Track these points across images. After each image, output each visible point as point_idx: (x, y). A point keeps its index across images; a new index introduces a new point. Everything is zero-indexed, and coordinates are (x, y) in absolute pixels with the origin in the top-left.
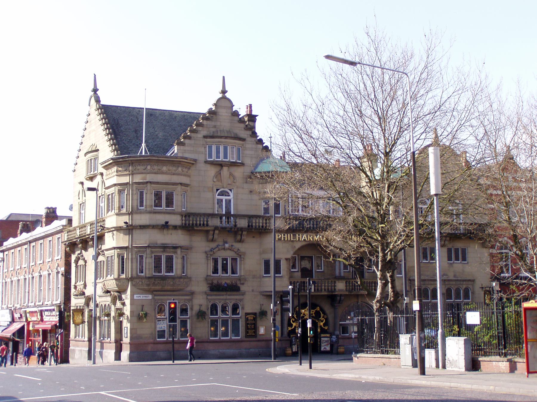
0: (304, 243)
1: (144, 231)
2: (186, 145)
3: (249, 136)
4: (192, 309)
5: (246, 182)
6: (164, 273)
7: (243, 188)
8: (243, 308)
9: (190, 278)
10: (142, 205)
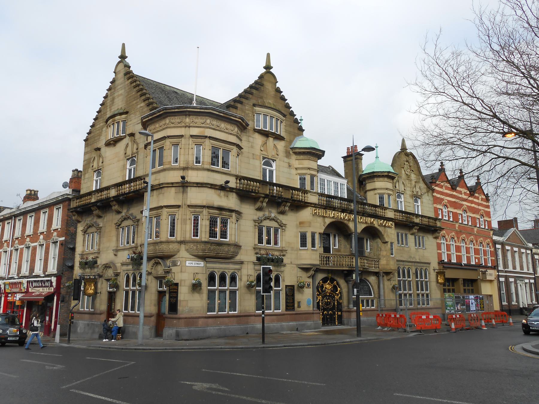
0: (333, 220)
1: (202, 189)
2: (238, 109)
8: (284, 280)
9: (240, 246)
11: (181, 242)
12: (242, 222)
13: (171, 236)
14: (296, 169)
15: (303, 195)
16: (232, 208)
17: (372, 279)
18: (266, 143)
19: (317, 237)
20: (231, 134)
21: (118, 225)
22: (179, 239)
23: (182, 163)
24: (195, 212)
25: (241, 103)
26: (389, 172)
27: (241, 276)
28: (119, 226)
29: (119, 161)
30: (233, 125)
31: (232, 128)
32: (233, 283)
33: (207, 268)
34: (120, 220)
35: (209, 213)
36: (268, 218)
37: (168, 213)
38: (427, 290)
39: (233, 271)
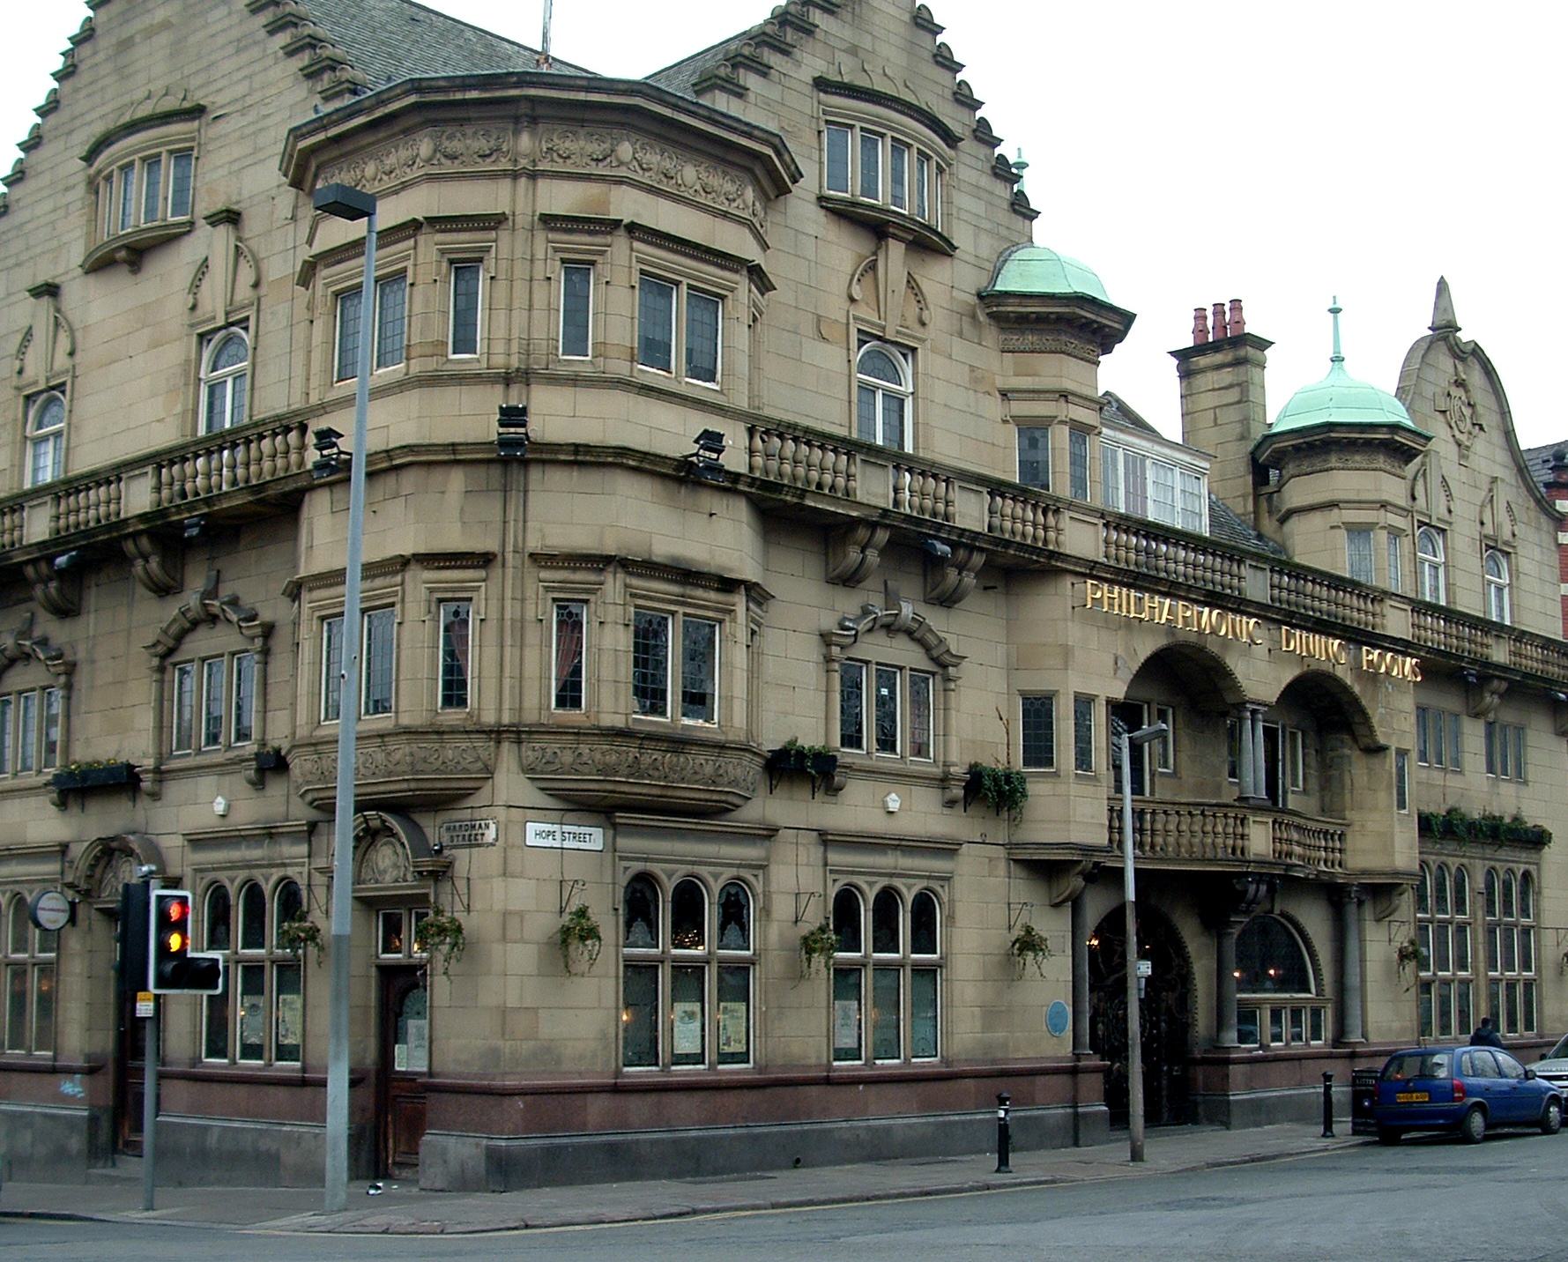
2: (751, 97)
3: (968, 133)
4: (766, 911)
5: (961, 335)
6: (674, 717)
7: (950, 357)
10: (576, 341)
11: (497, 734)
12: (772, 640)
13: (448, 701)
14: (1004, 394)
15: (1041, 518)
16: (731, 570)
17: (1314, 920)
18: (873, 267)
19: (1100, 715)
20: (725, 215)
21: (167, 655)
22: (489, 718)
23: (499, 347)
24: (563, 586)
25: (764, 71)
26: (1395, 428)
27: (767, 895)
28: (164, 657)
29: (156, 344)
30: (734, 173)
31: (729, 187)
32: (733, 930)
33: (621, 858)
34: (174, 629)
35: (633, 595)
36: (890, 628)
37: (431, 590)
38: (1527, 967)
39: (733, 872)
